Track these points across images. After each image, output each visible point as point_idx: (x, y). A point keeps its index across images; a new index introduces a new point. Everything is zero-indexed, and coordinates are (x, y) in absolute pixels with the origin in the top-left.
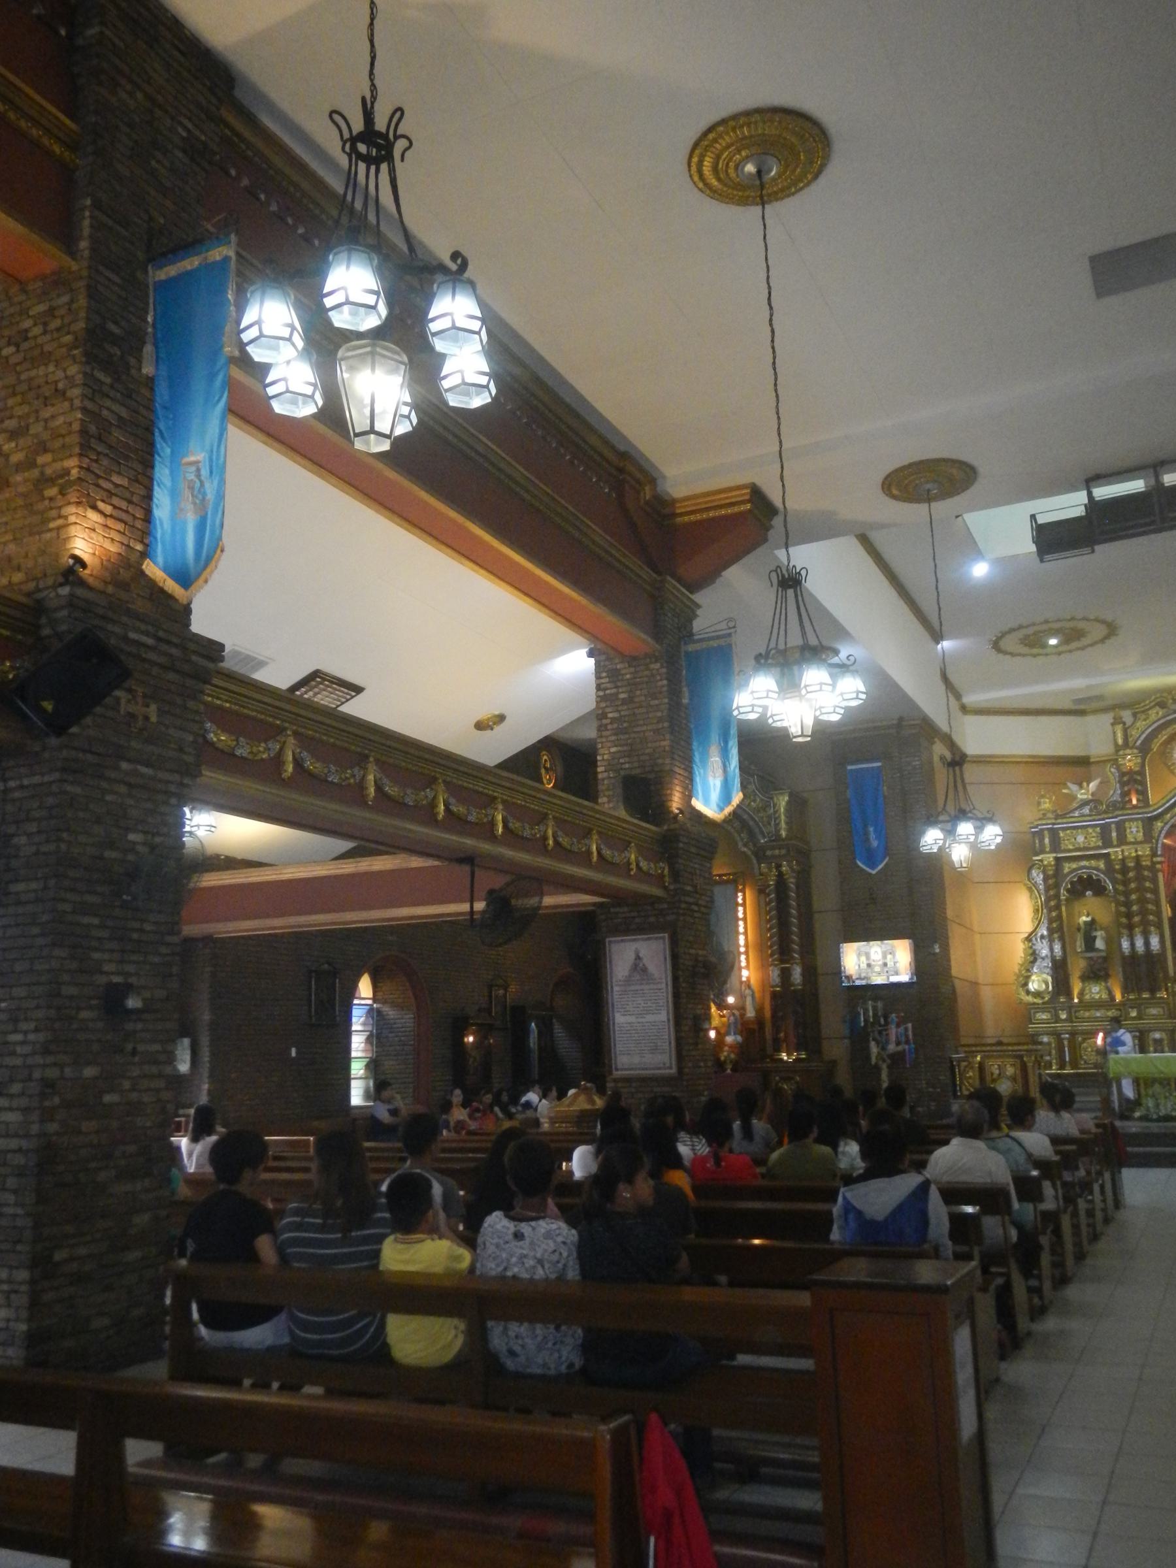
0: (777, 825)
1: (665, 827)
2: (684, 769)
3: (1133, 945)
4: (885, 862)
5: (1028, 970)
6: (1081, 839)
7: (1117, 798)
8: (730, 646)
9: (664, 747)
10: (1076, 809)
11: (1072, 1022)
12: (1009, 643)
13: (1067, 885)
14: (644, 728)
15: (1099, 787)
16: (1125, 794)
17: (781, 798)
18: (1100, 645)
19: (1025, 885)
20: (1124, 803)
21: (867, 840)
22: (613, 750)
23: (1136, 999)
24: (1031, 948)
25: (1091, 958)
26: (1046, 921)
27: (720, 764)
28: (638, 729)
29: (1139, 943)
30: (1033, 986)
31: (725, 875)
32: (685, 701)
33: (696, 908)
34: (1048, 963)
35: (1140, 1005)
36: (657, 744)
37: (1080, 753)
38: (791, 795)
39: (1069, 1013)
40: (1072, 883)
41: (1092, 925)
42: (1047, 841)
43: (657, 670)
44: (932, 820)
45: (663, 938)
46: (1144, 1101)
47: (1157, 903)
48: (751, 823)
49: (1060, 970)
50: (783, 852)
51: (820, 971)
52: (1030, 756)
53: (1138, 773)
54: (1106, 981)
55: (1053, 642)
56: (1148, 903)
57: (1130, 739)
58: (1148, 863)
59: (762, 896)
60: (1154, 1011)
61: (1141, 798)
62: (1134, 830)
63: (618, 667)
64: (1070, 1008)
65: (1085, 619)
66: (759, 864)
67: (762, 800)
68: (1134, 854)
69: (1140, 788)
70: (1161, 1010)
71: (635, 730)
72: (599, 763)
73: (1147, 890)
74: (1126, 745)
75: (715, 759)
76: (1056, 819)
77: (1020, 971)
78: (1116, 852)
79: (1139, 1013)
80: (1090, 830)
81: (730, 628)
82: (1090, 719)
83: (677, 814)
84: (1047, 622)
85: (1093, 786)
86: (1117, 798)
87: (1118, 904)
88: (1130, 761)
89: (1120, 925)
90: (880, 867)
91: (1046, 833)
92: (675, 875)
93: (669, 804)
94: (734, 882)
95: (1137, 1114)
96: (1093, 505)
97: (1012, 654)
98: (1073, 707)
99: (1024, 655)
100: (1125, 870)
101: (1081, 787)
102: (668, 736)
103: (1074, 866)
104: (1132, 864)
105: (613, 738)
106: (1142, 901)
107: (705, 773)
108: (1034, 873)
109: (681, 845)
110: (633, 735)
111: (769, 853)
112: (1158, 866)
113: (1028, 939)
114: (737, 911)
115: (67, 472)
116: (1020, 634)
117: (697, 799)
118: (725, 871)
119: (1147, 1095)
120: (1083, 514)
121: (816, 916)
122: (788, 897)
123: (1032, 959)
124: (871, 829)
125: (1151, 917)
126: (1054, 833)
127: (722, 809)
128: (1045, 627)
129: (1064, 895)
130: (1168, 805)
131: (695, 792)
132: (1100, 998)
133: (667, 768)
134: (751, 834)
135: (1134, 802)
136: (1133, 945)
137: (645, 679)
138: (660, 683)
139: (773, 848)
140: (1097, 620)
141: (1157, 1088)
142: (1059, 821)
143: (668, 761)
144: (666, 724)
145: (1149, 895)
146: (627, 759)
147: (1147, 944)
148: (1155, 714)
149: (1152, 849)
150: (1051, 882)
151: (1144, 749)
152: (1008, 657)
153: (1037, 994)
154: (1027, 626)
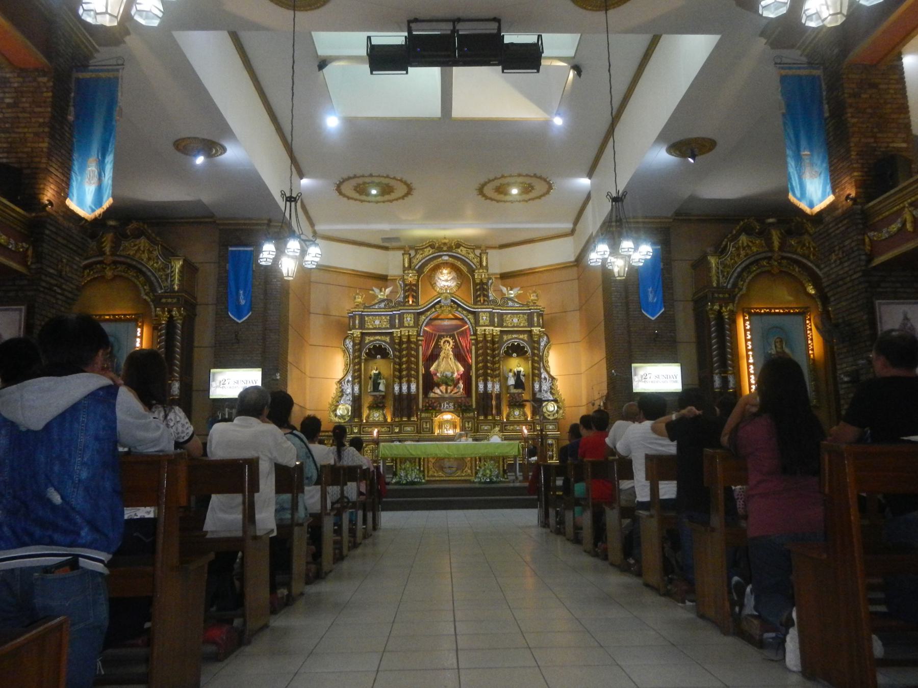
0: (172, 281)
1: (34, 214)
2: (63, 174)
3: (401, 388)
4: (248, 316)
5: (338, 402)
6: (377, 322)
7: (401, 299)
8: (117, 78)
9: (42, 148)
10: (376, 304)
11: (360, 434)
12: (346, 188)
13: (366, 350)
14: (26, 130)
15: (391, 292)
16: (406, 297)
17: (177, 263)
18: (401, 201)
19: (341, 348)
20: (404, 303)
21: (239, 302)
23: (397, 421)
24: (341, 387)
25: (373, 396)
26: (351, 372)
27: (96, 173)
28: (20, 130)
29: (405, 388)
30: (339, 412)
31: (129, 315)
32: (71, 118)
33: (59, 291)
34: (350, 397)
35: (401, 424)
36: (36, 145)
37: (384, 273)
38: (185, 261)
39: (359, 430)
40: (369, 349)
41: (378, 376)
42: (357, 322)
43: (44, 83)
44: (269, 239)
45: (20, 310)
46: (398, 472)
47: (417, 364)
48: (153, 278)
49: (357, 403)
50: (175, 300)
51: (194, 388)
52: (353, 270)
53: (414, 285)
54: (383, 410)
55: (374, 192)
56: (412, 363)
57: (413, 265)
58: (415, 340)
59: (156, 331)
60: (408, 429)
61: (415, 300)
62: (409, 319)
63: (8, 75)
64: (361, 425)
65: (394, 178)
66: (156, 308)
67: (163, 263)
68: (407, 334)
69: (415, 294)
70: (413, 428)
71: (17, 130)
73: (413, 356)
74: (410, 267)
75: (92, 168)
76: (364, 309)
77: (332, 402)
78: (396, 332)
79: (400, 430)
80: (384, 318)
81: (118, 65)
82: (391, 253)
83: (46, 206)
84: (371, 176)
85: (388, 291)
86: (401, 299)
87: (395, 363)
88: (411, 277)
89: (394, 376)
90: (244, 319)
91: (357, 316)
92: (38, 257)
93: (41, 196)
94: (136, 320)
95: (394, 481)
96: (411, 38)
97: (349, 198)
98: (381, 244)
99: (356, 200)
100: (401, 343)
101: (381, 291)
102: (47, 140)
103: (372, 339)
104: (405, 340)
106: (409, 362)
107: (82, 180)
108: (347, 341)
109: (47, 232)
110: (14, 135)
111: (164, 300)
112: (420, 342)
113: (340, 382)
114: (135, 342)
116: (354, 182)
118: (129, 312)
119: (400, 469)
120: (404, 43)
121: (196, 349)
122: (176, 333)
123: (340, 394)
124: (241, 292)
125: (413, 372)
126: (362, 317)
127: (93, 211)
128: (368, 180)
129: (364, 356)
130: (429, 306)
131: (71, 194)
132: (379, 420)
133: (44, 166)
134: (151, 285)
135: (411, 302)
136: (401, 388)
137: (31, 89)
138: (45, 94)
139: (166, 297)
140: (401, 181)
141: (408, 465)
142: (366, 310)
143: (44, 160)
145: (413, 359)
146: (5, 155)
147: (409, 388)
148: (429, 251)
149: (417, 331)
150: (357, 347)
151: (420, 271)
152: (345, 199)
153: (342, 417)
154: (359, 177)
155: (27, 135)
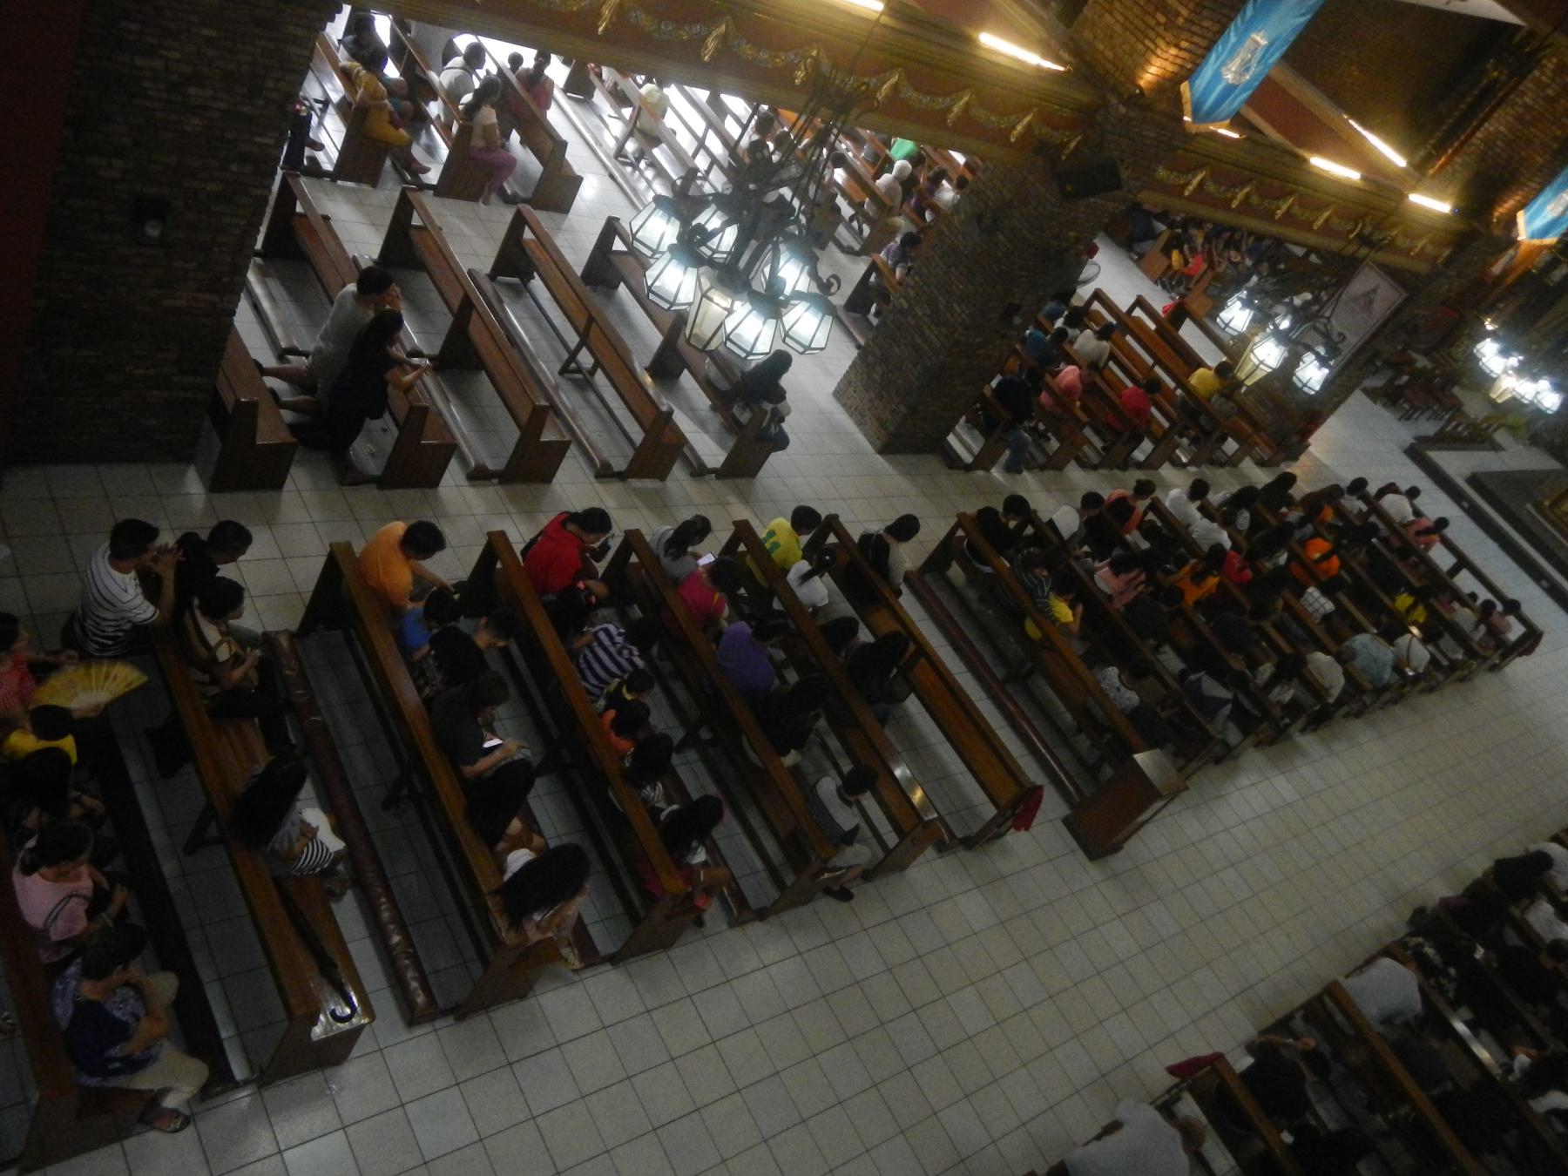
22: (1502, 129)
72: (1482, 129)
102: (1547, 157)
105: (1509, 118)
115: (1178, 14)
117: (1525, 213)
127: (1532, 237)
133: (1522, 179)
144: (1556, 146)
155: (1536, 140)
